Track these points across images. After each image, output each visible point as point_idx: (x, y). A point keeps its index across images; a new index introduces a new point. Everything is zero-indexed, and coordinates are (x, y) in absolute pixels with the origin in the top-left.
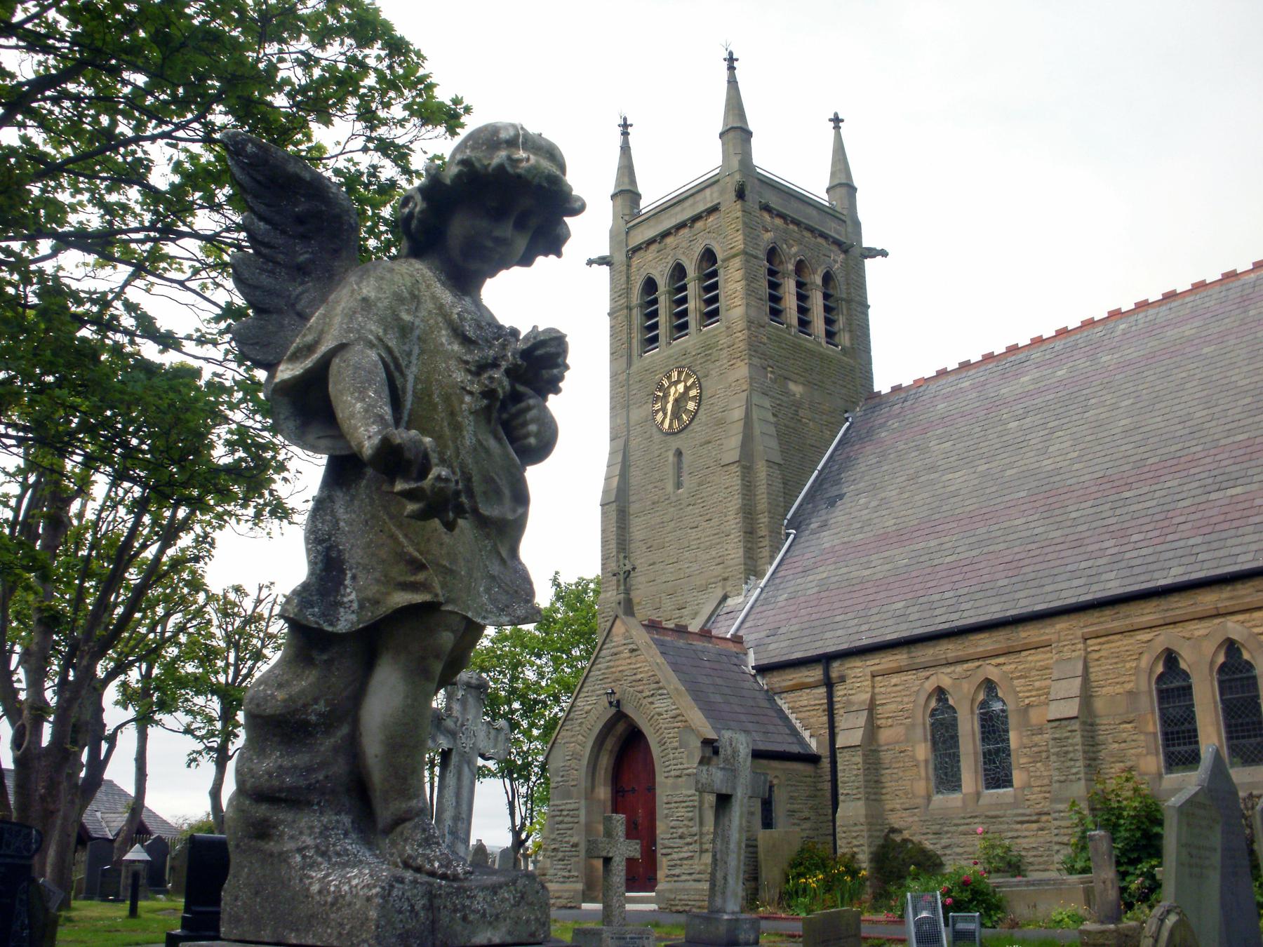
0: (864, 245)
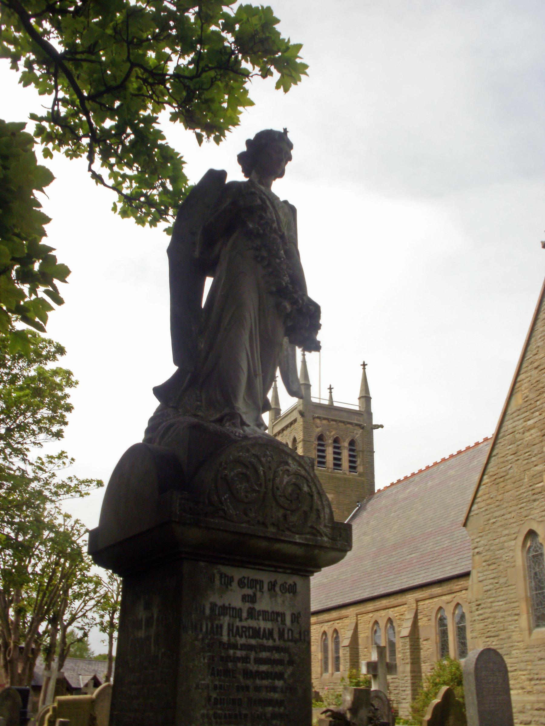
0: (374, 423)
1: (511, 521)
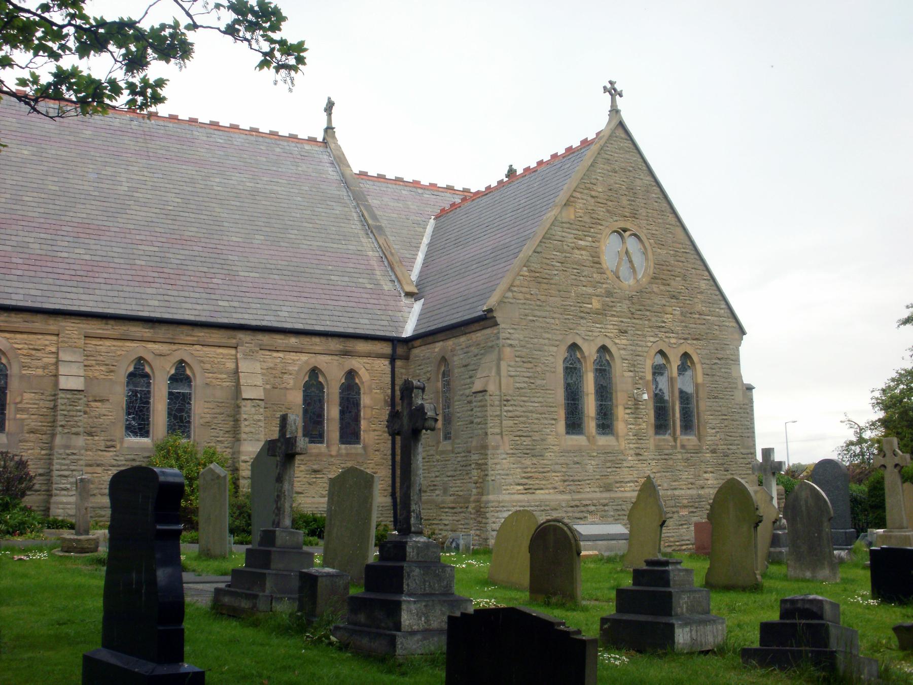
1: (554, 327)
